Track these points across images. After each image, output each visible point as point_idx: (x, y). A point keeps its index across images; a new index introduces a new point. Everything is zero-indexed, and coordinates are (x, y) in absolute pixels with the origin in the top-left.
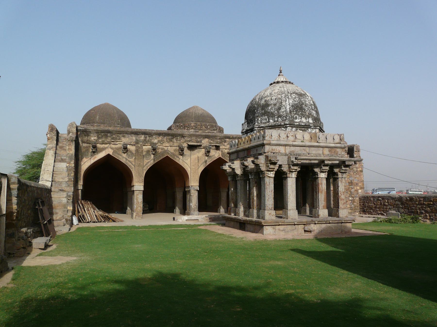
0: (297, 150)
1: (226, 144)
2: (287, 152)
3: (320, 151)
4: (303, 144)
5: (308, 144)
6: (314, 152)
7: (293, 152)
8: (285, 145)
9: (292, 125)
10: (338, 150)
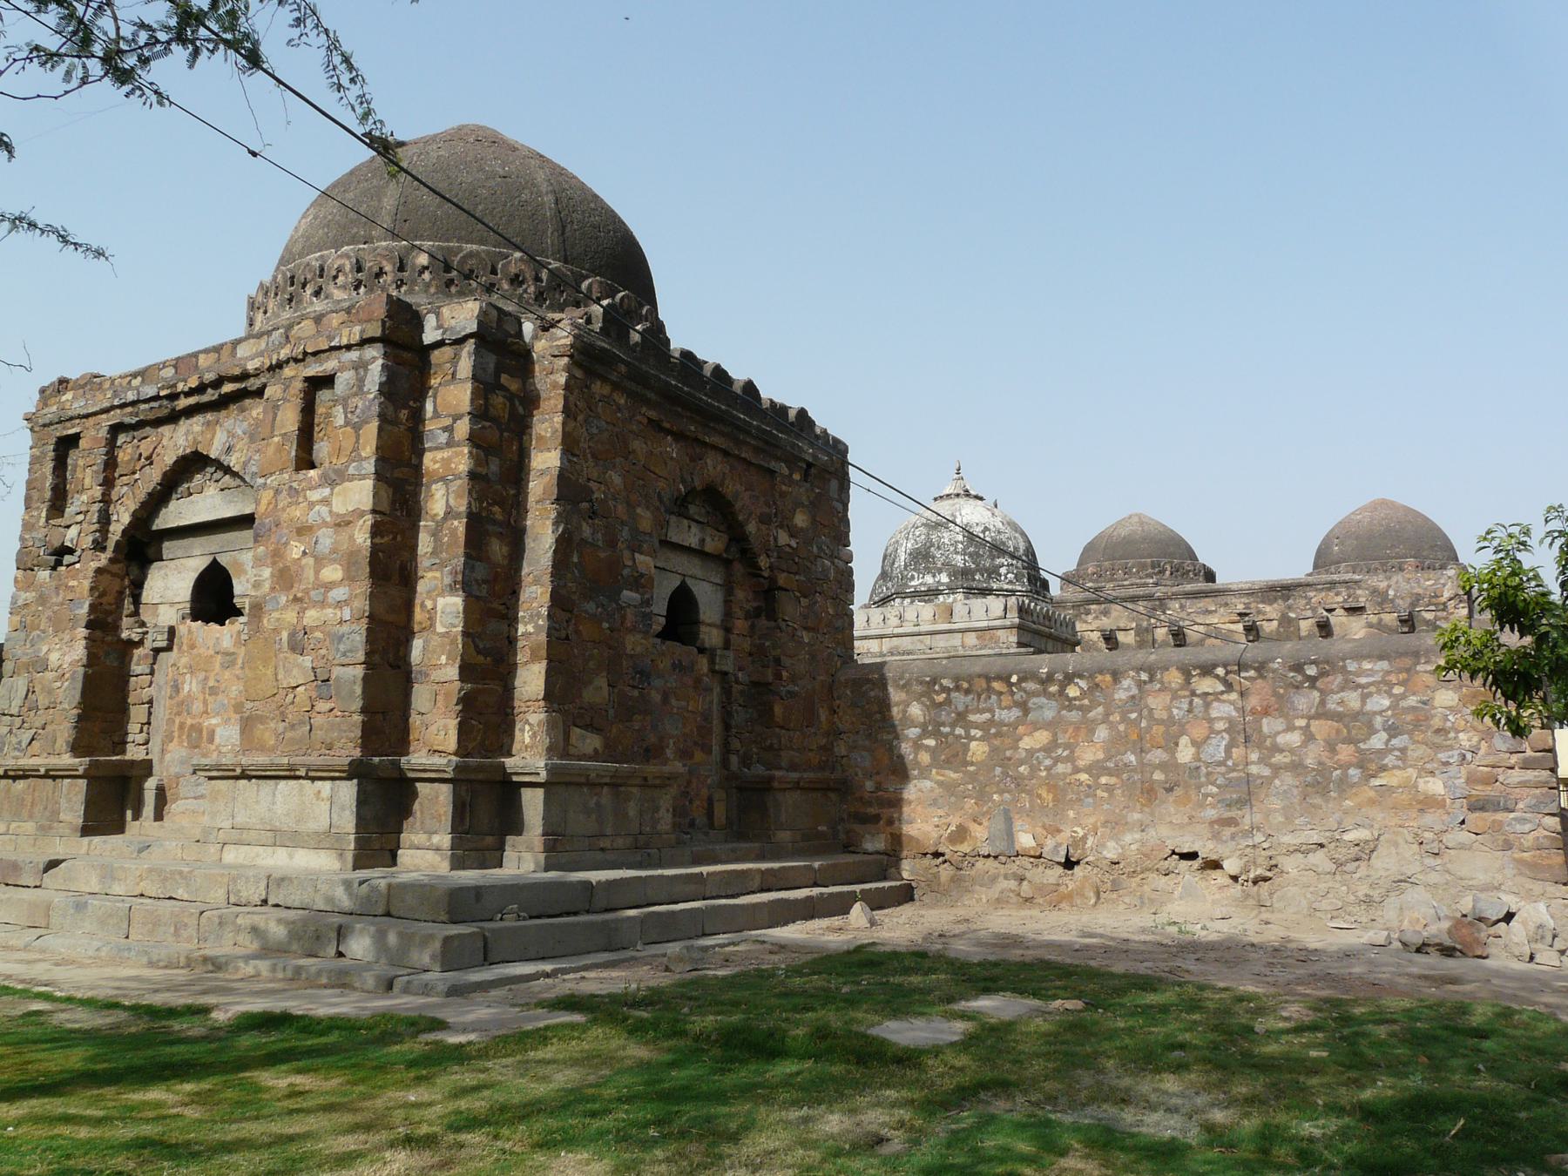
0: (906, 643)
1: (1090, 618)
2: (885, 650)
3: (956, 640)
4: (916, 629)
5: (924, 628)
6: (942, 644)
7: (897, 647)
8: (881, 637)
9: (902, 595)
10: (1000, 633)
